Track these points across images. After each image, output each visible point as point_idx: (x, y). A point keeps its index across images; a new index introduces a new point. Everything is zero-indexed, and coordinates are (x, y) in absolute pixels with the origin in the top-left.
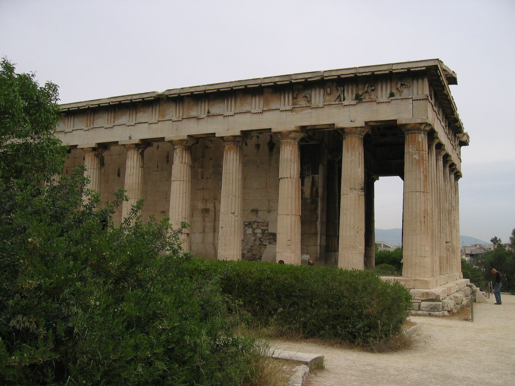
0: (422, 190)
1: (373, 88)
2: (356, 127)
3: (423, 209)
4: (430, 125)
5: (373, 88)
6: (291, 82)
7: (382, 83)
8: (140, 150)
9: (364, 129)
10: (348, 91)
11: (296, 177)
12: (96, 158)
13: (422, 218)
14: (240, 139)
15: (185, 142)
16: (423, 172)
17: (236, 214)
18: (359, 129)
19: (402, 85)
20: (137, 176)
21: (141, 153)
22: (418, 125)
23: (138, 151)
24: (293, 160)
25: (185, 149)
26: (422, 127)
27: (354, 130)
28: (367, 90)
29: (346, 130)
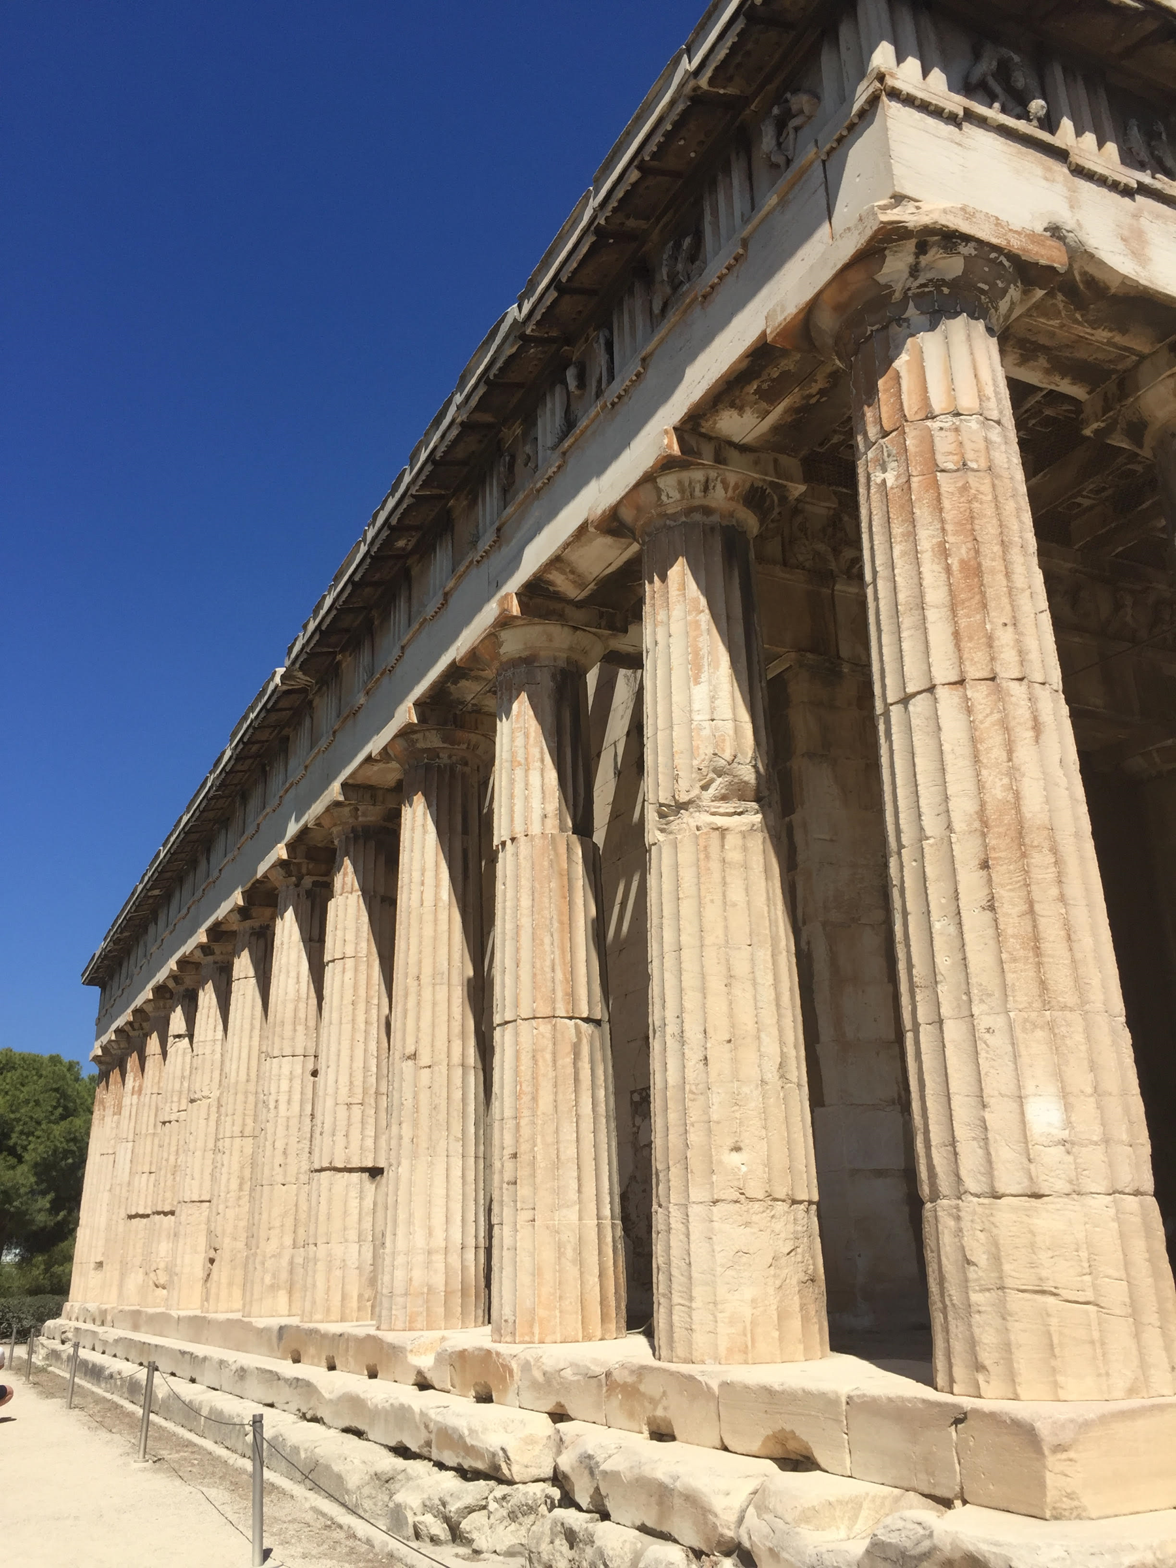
0: (943, 672)
1: (687, 241)
2: (648, 479)
3: (962, 808)
4: (950, 238)
5: (687, 241)
6: (462, 424)
7: (713, 185)
8: (308, 882)
9: (698, 475)
10: (621, 328)
11: (536, 829)
12: (253, 939)
13: (969, 879)
14: (433, 740)
15: (346, 810)
16: (943, 551)
17: (424, 1059)
18: (668, 482)
19: (781, 126)
20: (293, 974)
21: (309, 893)
22: (857, 277)
23: (297, 885)
24: (520, 757)
25: (356, 838)
26: (895, 267)
27: (646, 496)
28: (672, 276)
29: (627, 515)
